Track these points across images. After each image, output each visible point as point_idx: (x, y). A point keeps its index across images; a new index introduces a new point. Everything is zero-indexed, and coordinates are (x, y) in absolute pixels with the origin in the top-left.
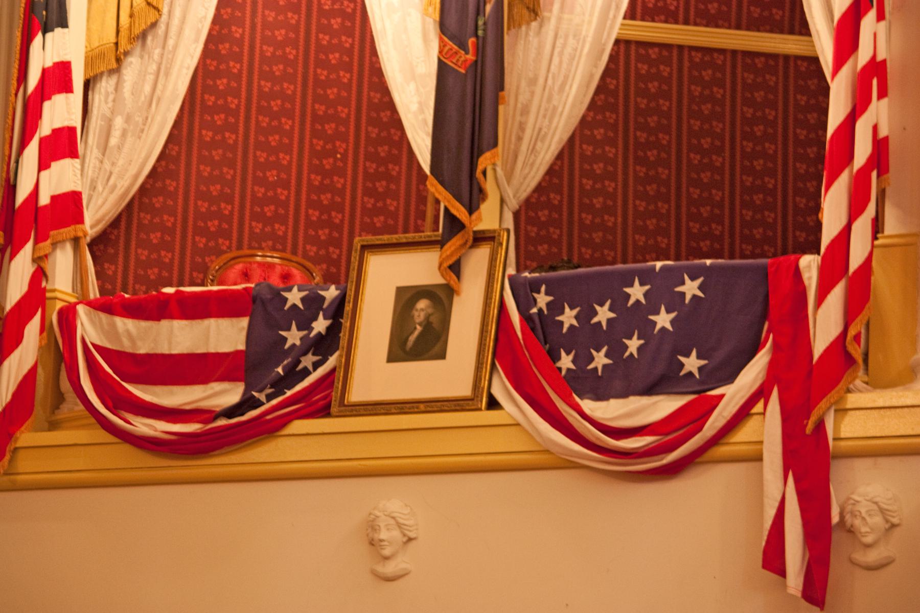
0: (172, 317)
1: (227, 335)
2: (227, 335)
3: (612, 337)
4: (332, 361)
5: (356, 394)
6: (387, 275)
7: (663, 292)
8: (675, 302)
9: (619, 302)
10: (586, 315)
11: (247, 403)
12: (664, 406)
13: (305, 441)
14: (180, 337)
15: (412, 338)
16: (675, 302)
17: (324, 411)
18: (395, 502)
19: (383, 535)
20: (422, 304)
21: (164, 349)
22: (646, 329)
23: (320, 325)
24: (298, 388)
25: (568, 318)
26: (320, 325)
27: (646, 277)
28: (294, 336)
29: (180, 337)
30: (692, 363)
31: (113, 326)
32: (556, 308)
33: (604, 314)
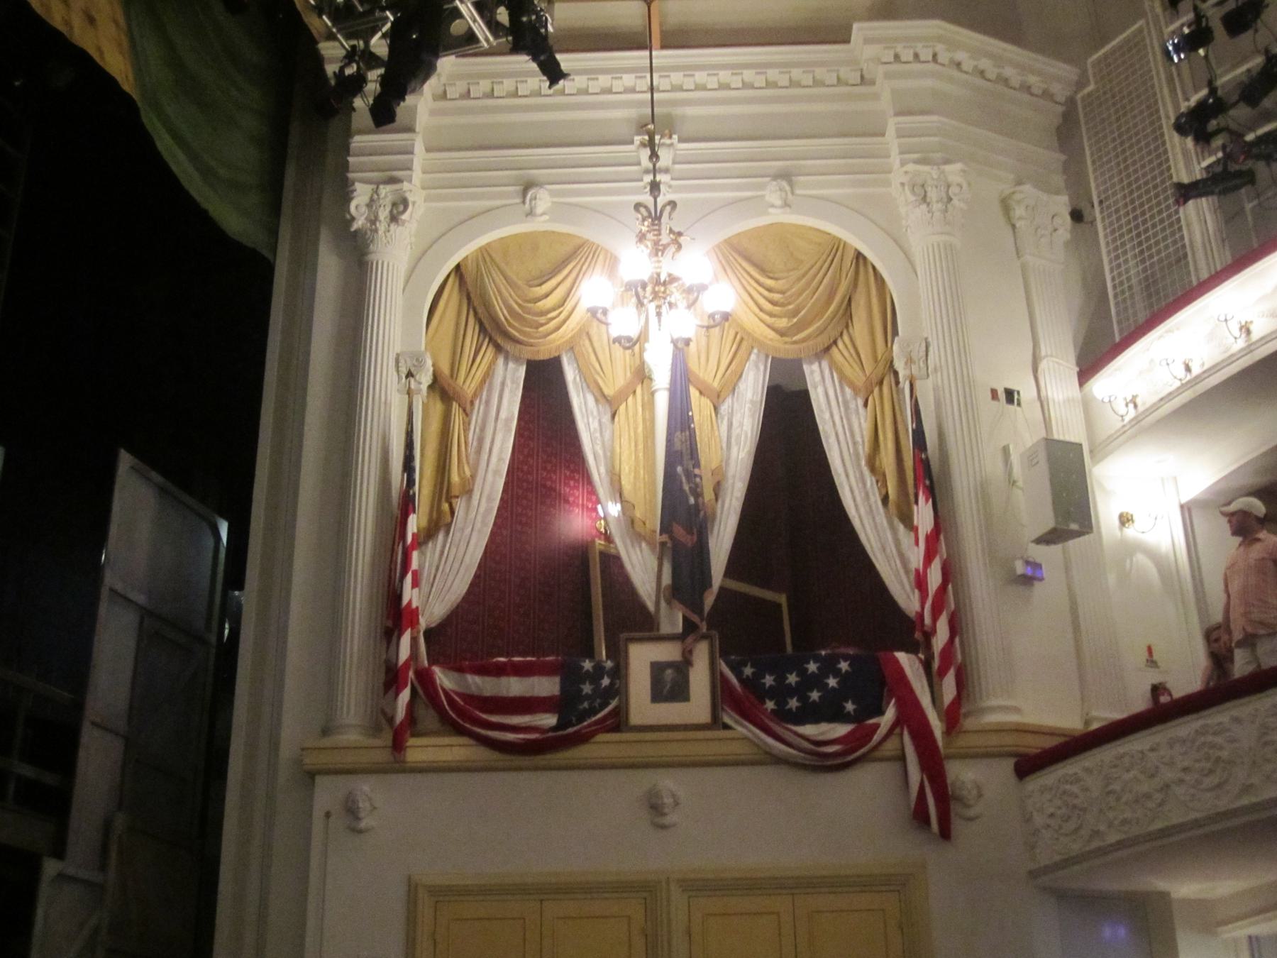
0: (508, 675)
1: (547, 686)
2: (547, 686)
3: (800, 691)
4: (614, 703)
5: (635, 718)
6: (642, 658)
7: (829, 666)
8: (837, 673)
9: (803, 673)
10: (781, 679)
11: (560, 726)
12: (841, 730)
13: (604, 746)
14: (515, 686)
15: (665, 691)
16: (837, 673)
17: (616, 728)
18: (667, 782)
19: (666, 800)
20: (669, 672)
21: (504, 693)
22: (823, 687)
23: (606, 681)
24: (599, 716)
25: (769, 680)
26: (606, 681)
27: (817, 659)
28: (587, 688)
29: (515, 686)
30: (850, 707)
31: (466, 681)
32: (758, 675)
33: (792, 679)
